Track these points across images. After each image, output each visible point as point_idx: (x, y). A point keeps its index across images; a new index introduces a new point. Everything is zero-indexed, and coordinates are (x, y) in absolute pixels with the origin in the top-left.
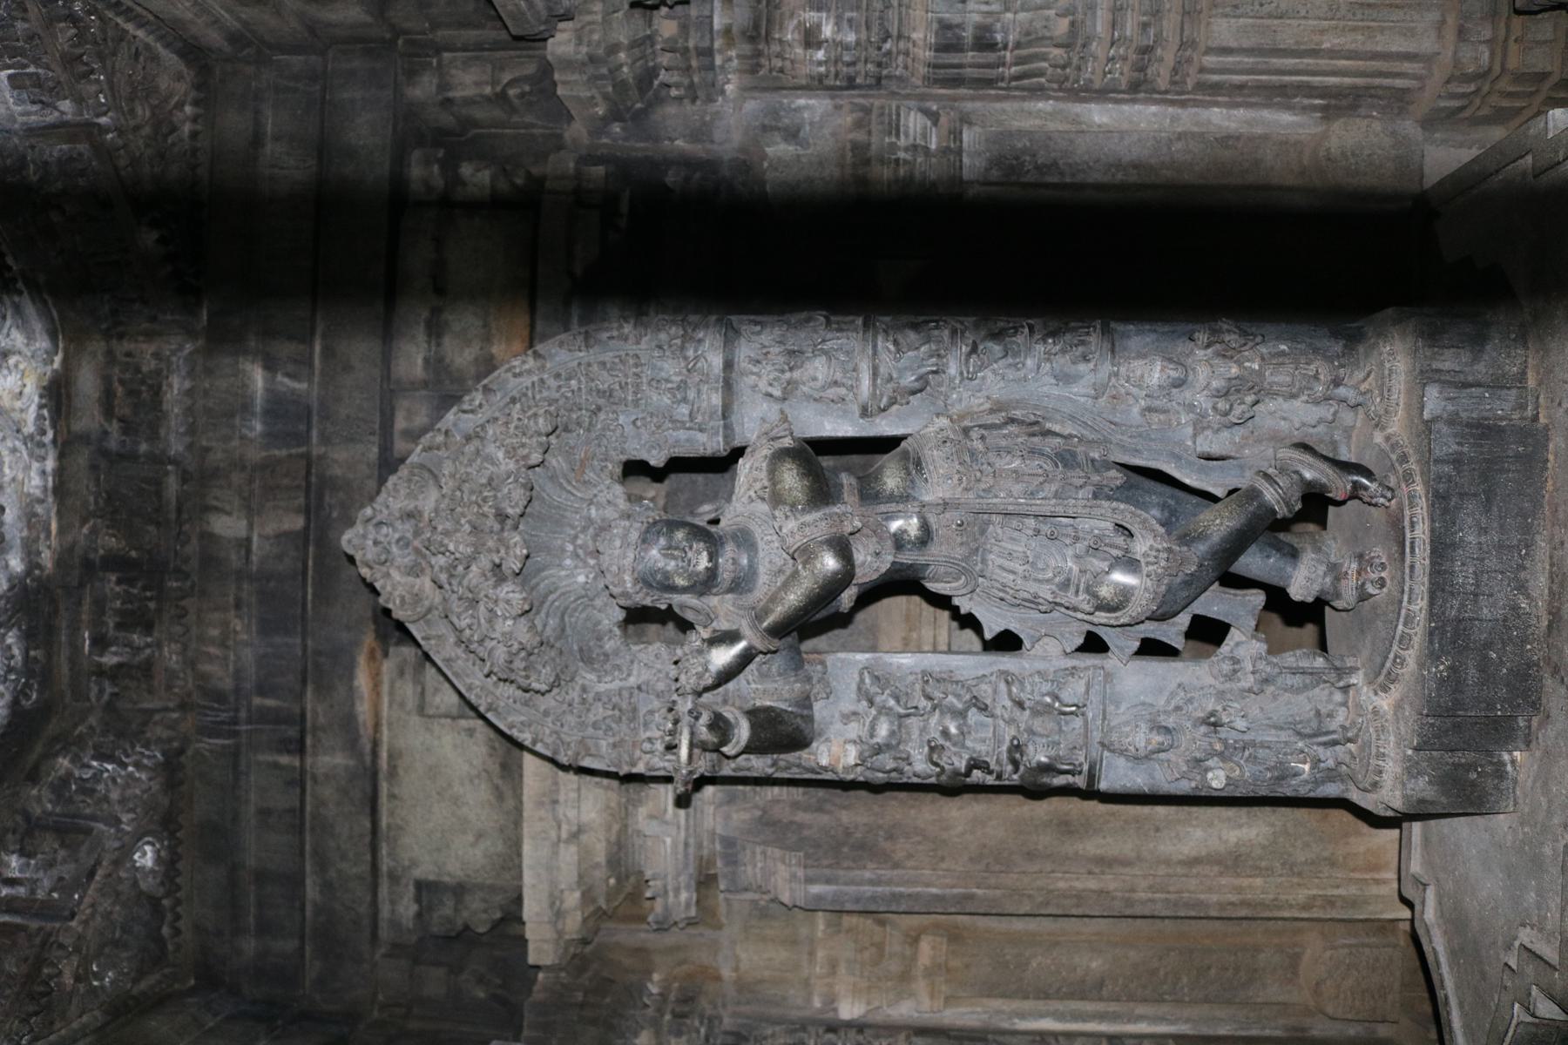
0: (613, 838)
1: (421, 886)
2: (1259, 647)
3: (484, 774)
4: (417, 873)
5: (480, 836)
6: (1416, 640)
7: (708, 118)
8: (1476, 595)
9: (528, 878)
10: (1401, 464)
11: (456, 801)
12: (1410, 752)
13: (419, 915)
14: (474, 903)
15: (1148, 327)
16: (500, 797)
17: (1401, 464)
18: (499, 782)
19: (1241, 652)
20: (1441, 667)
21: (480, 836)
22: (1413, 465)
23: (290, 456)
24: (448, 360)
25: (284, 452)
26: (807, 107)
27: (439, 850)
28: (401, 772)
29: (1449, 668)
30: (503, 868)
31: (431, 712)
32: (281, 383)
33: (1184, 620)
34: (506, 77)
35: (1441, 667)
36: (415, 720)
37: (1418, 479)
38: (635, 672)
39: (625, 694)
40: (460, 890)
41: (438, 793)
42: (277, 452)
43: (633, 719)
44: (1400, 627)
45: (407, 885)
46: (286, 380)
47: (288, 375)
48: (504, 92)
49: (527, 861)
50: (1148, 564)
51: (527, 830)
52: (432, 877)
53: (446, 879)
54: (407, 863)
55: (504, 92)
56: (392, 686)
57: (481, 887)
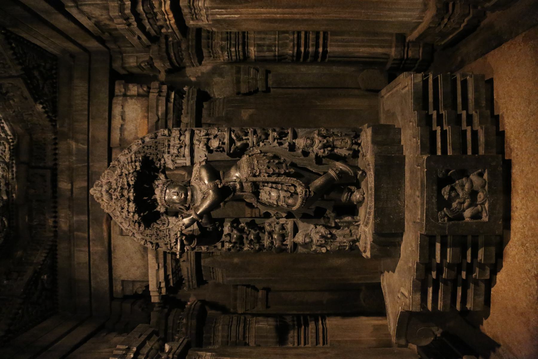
0: (173, 267)
1: (123, 281)
2: (333, 215)
3: (139, 251)
4: (122, 278)
5: (138, 267)
6: (372, 214)
7: (197, 71)
8: (387, 201)
9: (150, 279)
10: (368, 166)
11: (132, 258)
12: (372, 242)
13: (123, 289)
14: (138, 285)
15: (303, 129)
16: (144, 257)
17: (368, 166)
18: (143, 253)
19: (329, 216)
20: (378, 220)
21: (138, 267)
22: (371, 167)
23: (82, 166)
24: (126, 138)
25: (81, 165)
26: (224, 67)
27: (127, 272)
28: (116, 251)
29: (380, 221)
30: (145, 276)
31: (124, 234)
32: (80, 146)
33: (313, 207)
34: (141, 60)
35: (378, 220)
36: (120, 236)
37: (372, 170)
38: (170, 225)
39: (168, 230)
40: (133, 282)
41: (127, 257)
42: (79, 165)
43: (170, 238)
44: (368, 210)
45: (119, 282)
46: (81, 145)
47: (82, 144)
48: (140, 65)
49: (150, 275)
50: (300, 194)
51: (149, 266)
52: (126, 279)
53: (130, 280)
54: (119, 276)
55: (140, 65)
56: (113, 227)
57: (139, 281)
